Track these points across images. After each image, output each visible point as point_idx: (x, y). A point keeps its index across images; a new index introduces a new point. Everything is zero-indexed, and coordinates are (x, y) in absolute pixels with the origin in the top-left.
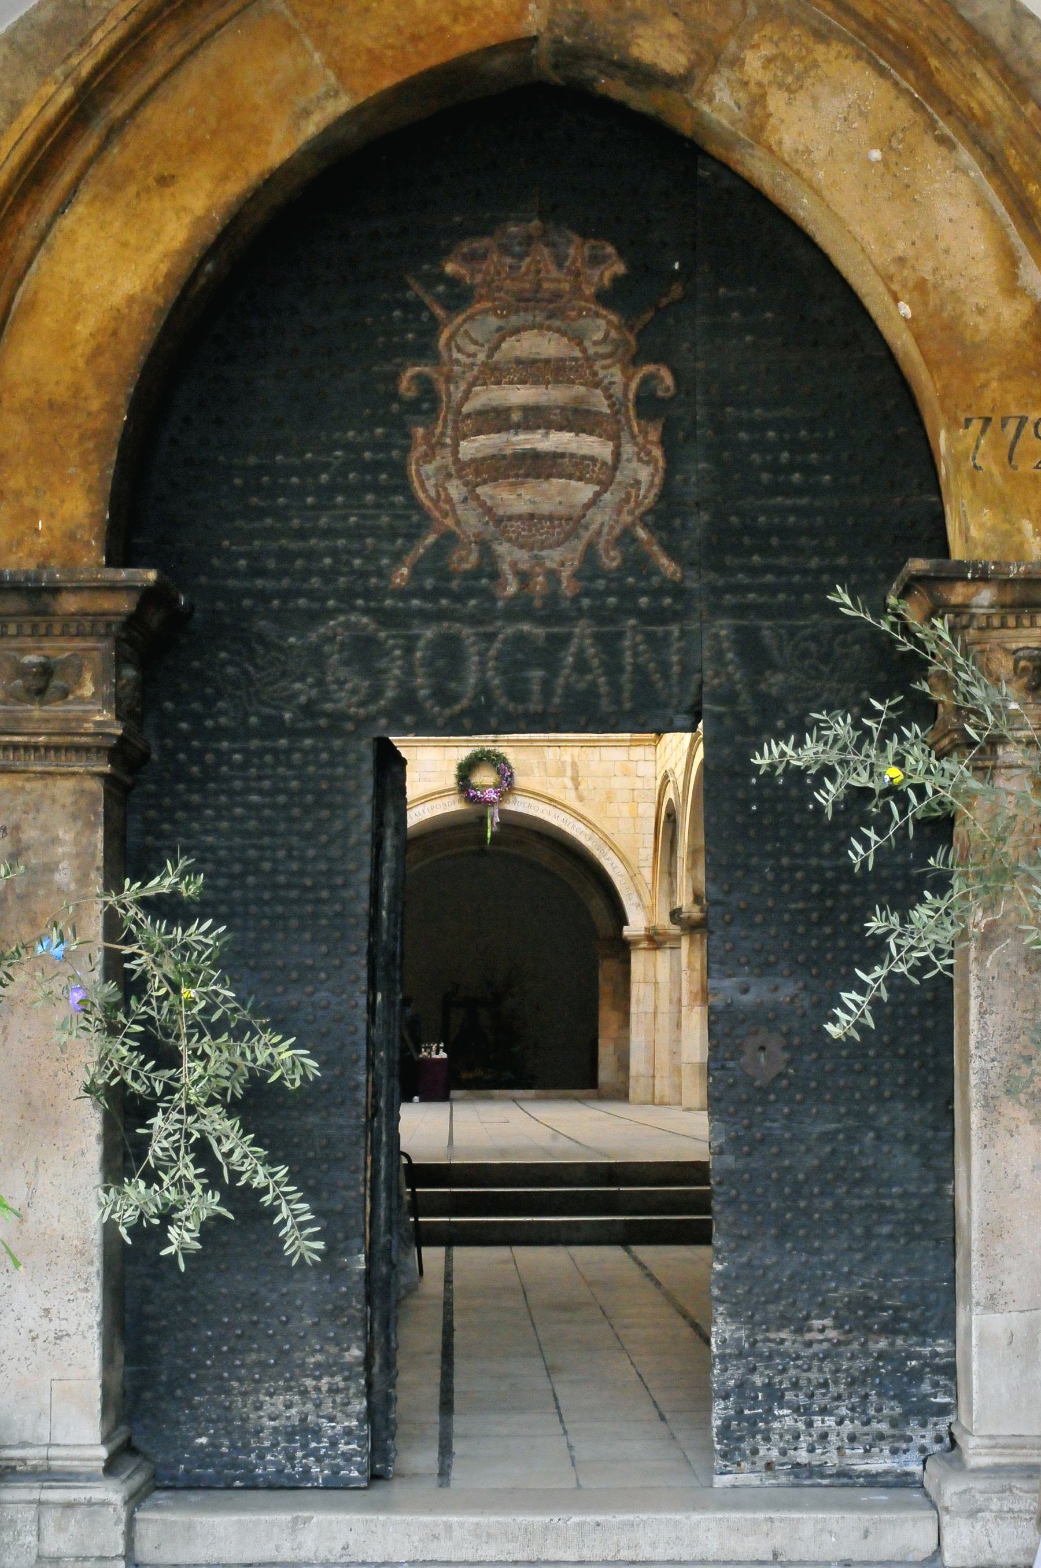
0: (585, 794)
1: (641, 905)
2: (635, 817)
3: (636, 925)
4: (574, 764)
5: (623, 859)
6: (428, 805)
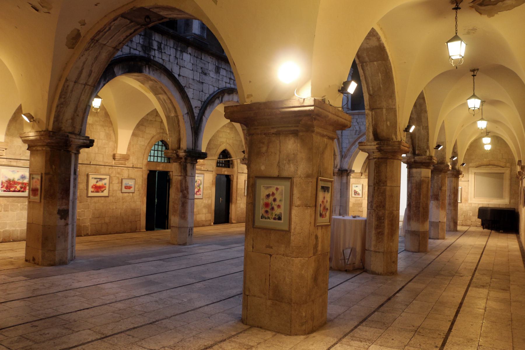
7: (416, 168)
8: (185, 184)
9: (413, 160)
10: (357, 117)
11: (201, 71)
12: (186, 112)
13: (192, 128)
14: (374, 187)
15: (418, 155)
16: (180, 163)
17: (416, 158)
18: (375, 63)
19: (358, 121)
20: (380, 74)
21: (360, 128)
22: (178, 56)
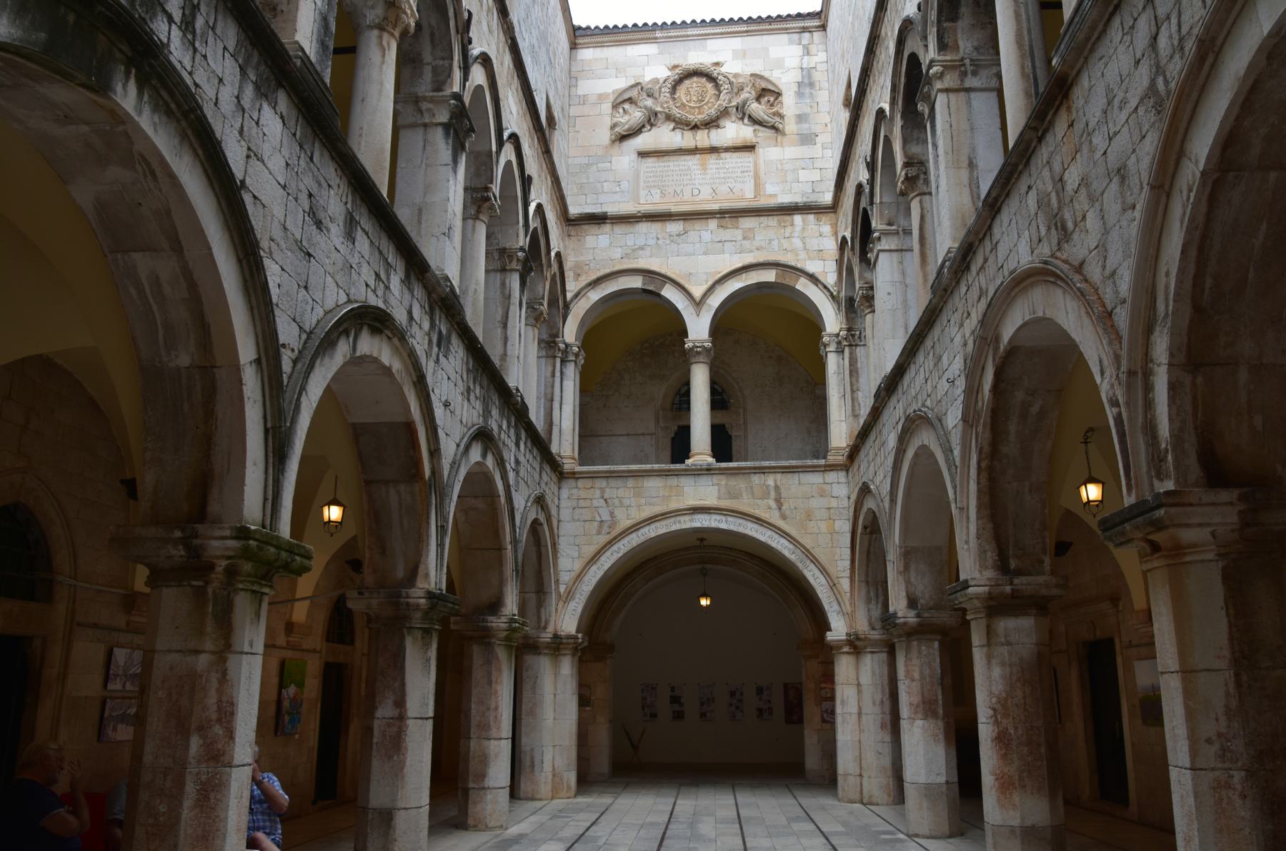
0: (788, 513)
1: (842, 612)
2: (832, 533)
3: (838, 629)
4: (777, 488)
5: (823, 571)
6: (653, 526)
7: (1016, 616)
8: (220, 692)
9: (1008, 589)
10: (603, 483)
11: (307, 209)
12: (255, 357)
13: (266, 431)
14: (1237, 675)
15: (1019, 572)
16: (200, 593)
17: (1016, 581)
18: (1273, 176)
20: (1264, 227)
21: (612, 514)
22: (246, 102)
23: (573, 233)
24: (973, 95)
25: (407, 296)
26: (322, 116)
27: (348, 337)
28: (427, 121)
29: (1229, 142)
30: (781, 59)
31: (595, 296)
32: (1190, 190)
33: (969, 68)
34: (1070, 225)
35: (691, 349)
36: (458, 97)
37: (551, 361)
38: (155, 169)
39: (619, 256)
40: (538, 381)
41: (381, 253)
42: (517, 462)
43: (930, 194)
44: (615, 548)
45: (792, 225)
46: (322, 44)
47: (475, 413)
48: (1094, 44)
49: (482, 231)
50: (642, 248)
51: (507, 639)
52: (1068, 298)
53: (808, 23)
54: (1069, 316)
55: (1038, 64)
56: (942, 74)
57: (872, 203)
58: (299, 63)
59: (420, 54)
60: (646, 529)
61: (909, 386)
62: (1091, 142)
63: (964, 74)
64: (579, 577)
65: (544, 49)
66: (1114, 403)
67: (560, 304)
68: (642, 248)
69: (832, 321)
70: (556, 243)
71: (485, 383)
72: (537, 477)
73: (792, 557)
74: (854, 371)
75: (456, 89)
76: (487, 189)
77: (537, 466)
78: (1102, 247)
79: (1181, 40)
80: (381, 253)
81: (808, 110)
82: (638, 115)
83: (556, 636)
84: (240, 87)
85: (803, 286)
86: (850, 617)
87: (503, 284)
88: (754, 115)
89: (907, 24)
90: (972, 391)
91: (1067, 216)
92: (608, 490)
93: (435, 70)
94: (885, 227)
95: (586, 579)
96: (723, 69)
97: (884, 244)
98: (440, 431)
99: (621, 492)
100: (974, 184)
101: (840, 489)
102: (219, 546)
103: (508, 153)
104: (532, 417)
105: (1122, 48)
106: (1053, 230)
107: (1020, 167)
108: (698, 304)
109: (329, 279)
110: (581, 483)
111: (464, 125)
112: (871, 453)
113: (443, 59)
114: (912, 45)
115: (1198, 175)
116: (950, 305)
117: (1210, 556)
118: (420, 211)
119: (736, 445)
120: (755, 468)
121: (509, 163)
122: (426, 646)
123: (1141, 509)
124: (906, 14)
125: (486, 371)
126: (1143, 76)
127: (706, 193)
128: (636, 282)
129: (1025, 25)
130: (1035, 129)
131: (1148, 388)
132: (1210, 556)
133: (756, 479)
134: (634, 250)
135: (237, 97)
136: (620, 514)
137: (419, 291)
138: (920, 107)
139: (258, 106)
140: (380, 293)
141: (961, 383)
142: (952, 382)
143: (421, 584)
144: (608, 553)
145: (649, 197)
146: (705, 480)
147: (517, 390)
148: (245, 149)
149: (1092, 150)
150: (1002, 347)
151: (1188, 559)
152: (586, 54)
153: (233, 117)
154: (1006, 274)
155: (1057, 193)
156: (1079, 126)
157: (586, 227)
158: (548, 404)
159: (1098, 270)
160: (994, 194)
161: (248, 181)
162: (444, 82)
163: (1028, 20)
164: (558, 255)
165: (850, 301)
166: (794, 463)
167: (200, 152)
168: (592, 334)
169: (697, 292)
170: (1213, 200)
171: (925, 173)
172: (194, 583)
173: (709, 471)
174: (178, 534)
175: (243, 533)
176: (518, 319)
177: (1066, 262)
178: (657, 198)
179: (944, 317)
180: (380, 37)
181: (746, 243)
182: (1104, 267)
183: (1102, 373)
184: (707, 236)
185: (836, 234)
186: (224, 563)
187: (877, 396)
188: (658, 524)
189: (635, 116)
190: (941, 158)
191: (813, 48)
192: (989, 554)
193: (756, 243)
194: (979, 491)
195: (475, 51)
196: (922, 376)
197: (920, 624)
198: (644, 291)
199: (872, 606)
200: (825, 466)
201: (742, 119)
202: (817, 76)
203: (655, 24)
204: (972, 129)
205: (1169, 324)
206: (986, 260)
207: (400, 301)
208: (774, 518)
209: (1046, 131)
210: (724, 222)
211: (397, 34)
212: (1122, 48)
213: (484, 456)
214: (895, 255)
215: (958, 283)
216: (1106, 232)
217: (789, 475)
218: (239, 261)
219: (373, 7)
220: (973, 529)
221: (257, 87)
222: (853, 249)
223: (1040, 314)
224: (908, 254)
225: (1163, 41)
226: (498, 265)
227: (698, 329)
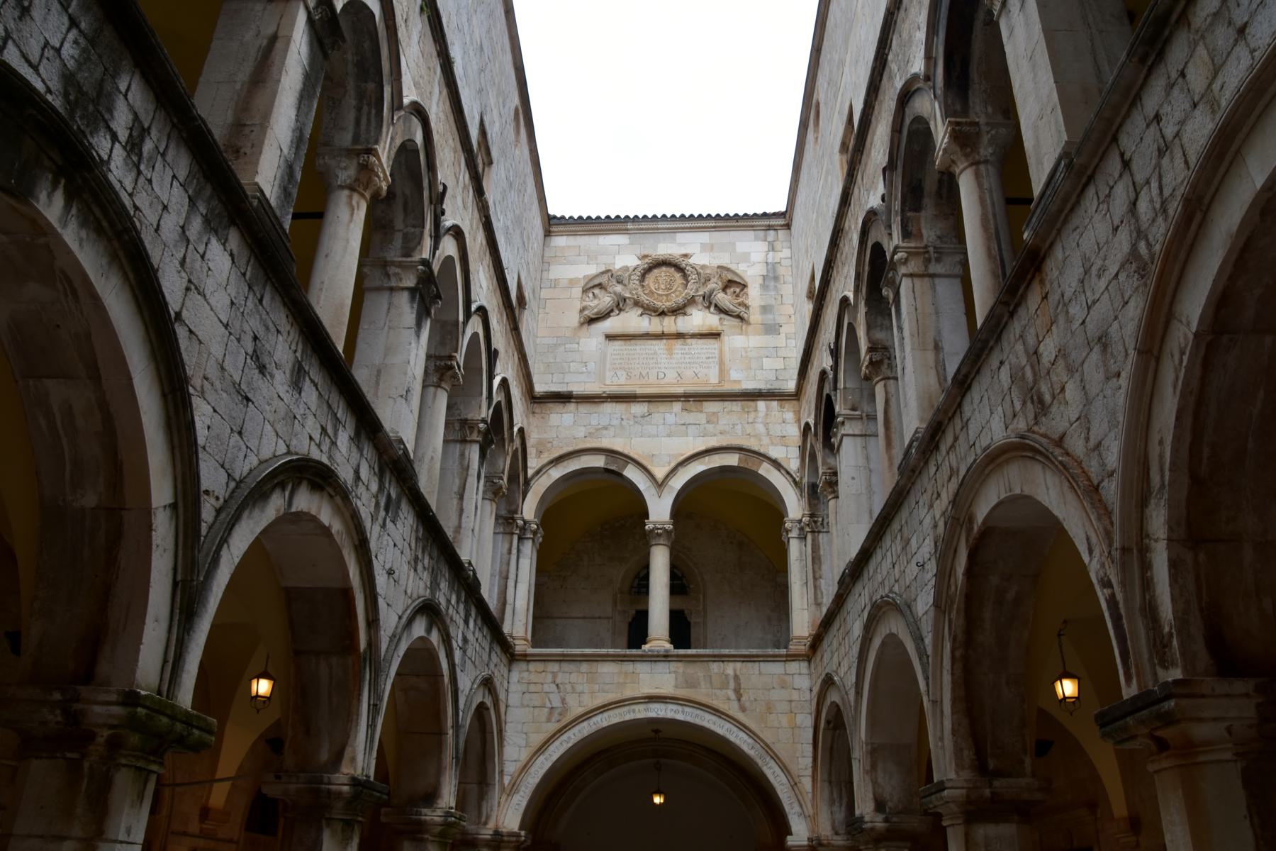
0: (747, 704)
1: (802, 814)
2: (794, 727)
4: (736, 677)
5: (785, 769)
6: (606, 715)
9: (987, 792)
10: (554, 667)
11: (250, 351)
13: (175, 584)
15: (998, 774)
17: (996, 783)
18: (1268, 340)
19: (558, 681)
21: (563, 700)
23: (537, 410)
24: (937, 281)
25: (355, 454)
26: (279, 262)
27: (284, 490)
28: (393, 284)
29: (1223, 303)
30: (749, 255)
31: (556, 473)
32: (1182, 353)
33: (933, 256)
34: (1047, 398)
35: (652, 531)
36: (426, 263)
37: (508, 537)
38: (75, 286)
39: (582, 434)
40: (494, 558)
41: (329, 407)
42: (465, 640)
43: (896, 379)
44: (564, 737)
45: (756, 410)
46: (285, 191)
47: (422, 584)
48: (1067, 216)
49: (442, 400)
50: (605, 428)
51: (442, 835)
52: (1049, 474)
53: (773, 222)
54: (1050, 493)
55: (1003, 246)
56: (906, 259)
57: (835, 389)
58: (255, 203)
59: (391, 221)
60: (598, 718)
61: (875, 571)
62: (1067, 312)
63: (927, 261)
64: (525, 768)
65: (518, 232)
66: (1106, 584)
67: (519, 480)
68: (605, 428)
69: (795, 506)
70: (519, 419)
71: (435, 554)
72: (485, 657)
73: (751, 753)
74: (816, 559)
75: (426, 255)
76: (451, 358)
77: (486, 645)
78: (1084, 419)
79: (1163, 203)
80: (329, 407)
81: (773, 302)
82: (605, 302)
83: (497, 833)
84: (187, 218)
85: (766, 470)
86: (813, 819)
87: (462, 455)
88: (721, 304)
89: (871, 215)
90: (944, 575)
91: (1044, 388)
92: (560, 675)
93: (406, 238)
94: (849, 412)
95: (532, 770)
96: (691, 261)
97: (848, 429)
98: (380, 601)
99: (574, 678)
100: (940, 367)
101: (800, 681)
102: (102, 710)
103: (475, 325)
104: (484, 592)
105: (1097, 217)
106: (1029, 404)
107: (991, 343)
108: (660, 485)
109: (268, 427)
110: (532, 666)
111: (432, 292)
112: (835, 644)
113: (414, 226)
114: (876, 235)
115: (1191, 337)
116: (918, 487)
117: (1228, 755)
118: (379, 372)
119: (695, 633)
120: (714, 656)
121: (475, 335)
122: (346, 841)
123: (1145, 701)
124: (869, 206)
125: (436, 541)
126: (1123, 242)
127: (671, 376)
128: (599, 462)
129: (990, 209)
130: (1007, 304)
131: (1146, 566)
132: (1228, 755)
133: (715, 667)
134: (597, 430)
135: (183, 227)
136: (572, 701)
137: (368, 451)
138: (884, 292)
139: (205, 240)
140: (325, 448)
141: (932, 568)
142: (922, 566)
143: (346, 769)
144: (557, 743)
145: (615, 379)
146: (661, 667)
147: (470, 563)
148: (185, 280)
149: (1069, 321)
150: (976, 528)
151: (1201, 758)
152: (560, 241)
153: (175, 246)
154: (979, 451)
155: (1032, 367)
156: (1053, 298)
157: (551, 405)
158: (503, 582)
159: (1081, 442)
160: (964, 371)
161: (185, 314)
162: (414, 249)
163: (993, 205)
164: (521, 430)
165: (813, 487)
166: (754, 651)
167: (131, 276)
168: (552, 511)
169: (660, 473)
170: (1207, 364)
171: (889, 359)
172: (69, 755)
173: (666, 657)
174: (57, 696)
175: (131, 699)
176: (475, 490)
177: (1044, 436)
178: (623, 380)
179: (912, 499)
180: (350, 197)
181: (710, 427)
182: (1087, 439)
183: (1091, 552)
184: (670, 418)
185: (799, 421)
186: (106, 733)
187: (841, 582)
188: (611, 713)
189: (605, 300)
190: (907, 341)
191: (778, 245)
192: (966, 752)
193: (720, 427)
194: (953, 682)
195: (448, 222)
196: (889, 560)
197: (888, 830)
198: (607, 471)
199: (835, 808)
200: (787, 656)
201: (708, 307)
202: (781, 271)
203: (627, 217)
204: (937, 313)
205: (1166, 496)
206: (956, 439)
207: (347, 458)
208: (733, 709)
209: (1018, 305)
210: (688, 405)
211: (368, 195)
212: (1097, 217)
213: (429, 631)
214: (859, 439)
215: (926, 463)
216: (1088, 402)
217: (750, 664)
218: (164, 395)
219: (345, 169)
220: (948, 724)
221: (207, 221)
222: (816, 434)
223: (1018, 491)
224: (872, 440)
225: (1143, 206)
226: (458, 436)
227: (660, 510)
